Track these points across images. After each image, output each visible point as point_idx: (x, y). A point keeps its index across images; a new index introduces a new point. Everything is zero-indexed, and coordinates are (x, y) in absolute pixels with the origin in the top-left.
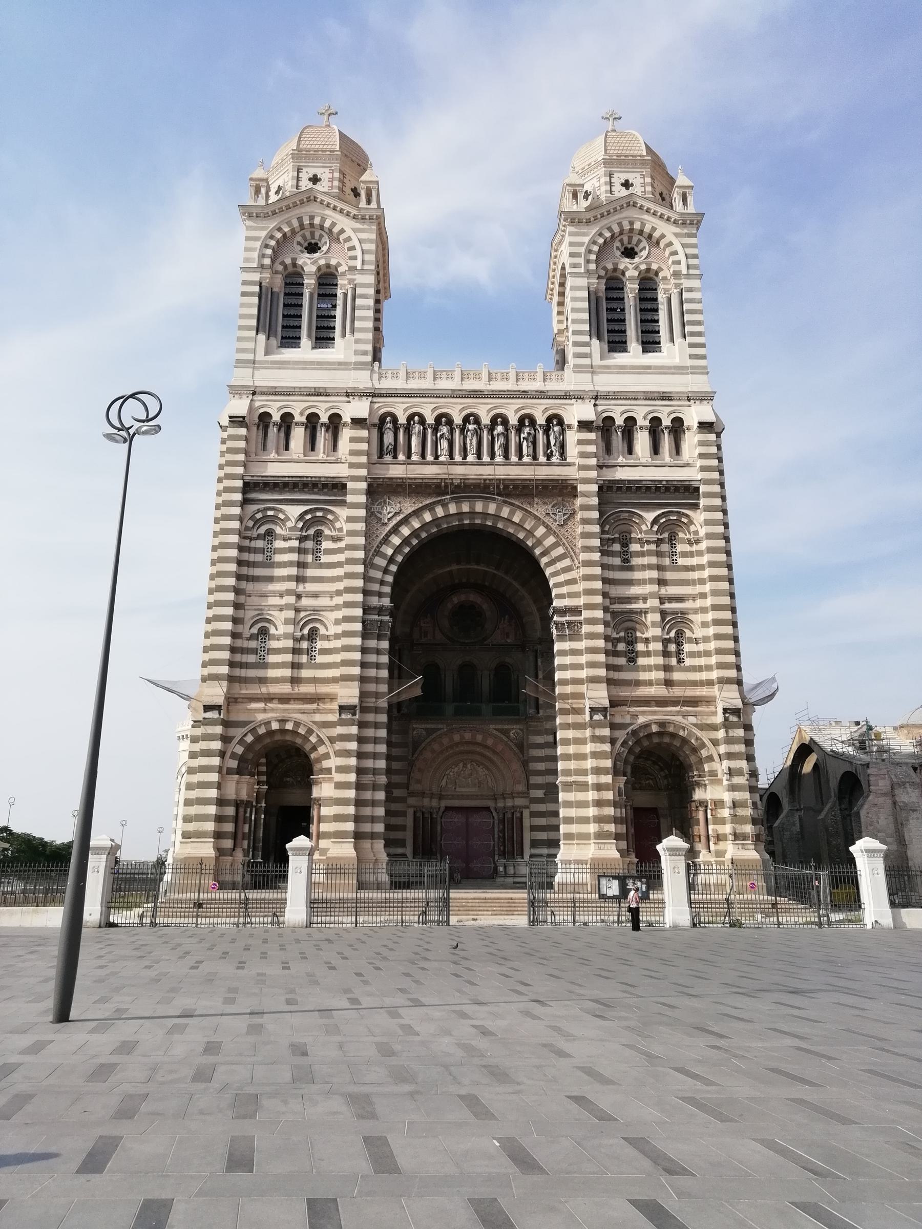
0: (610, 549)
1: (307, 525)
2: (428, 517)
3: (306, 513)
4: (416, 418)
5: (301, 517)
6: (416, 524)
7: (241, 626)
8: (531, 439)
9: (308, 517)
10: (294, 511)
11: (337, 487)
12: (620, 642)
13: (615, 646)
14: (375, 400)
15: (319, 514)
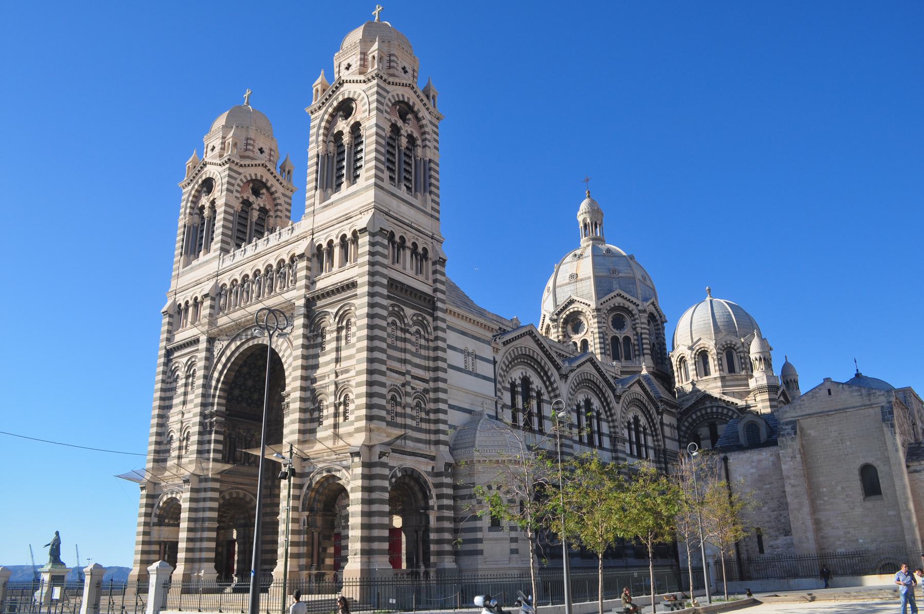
0: (315, 342)
1: (189, 369)
2: (233, 347)
3: (188, 360)
4: (234, 282)
5: (187, 363)
6: (228, 353)
7: (163, 437)
8: (282, 276)
9: (189, 363)
10: (184, 360)
11: (196, 341)
12: (315, 411)
13: (311, 415)
14: (219, 278)
15: (193, 360)
